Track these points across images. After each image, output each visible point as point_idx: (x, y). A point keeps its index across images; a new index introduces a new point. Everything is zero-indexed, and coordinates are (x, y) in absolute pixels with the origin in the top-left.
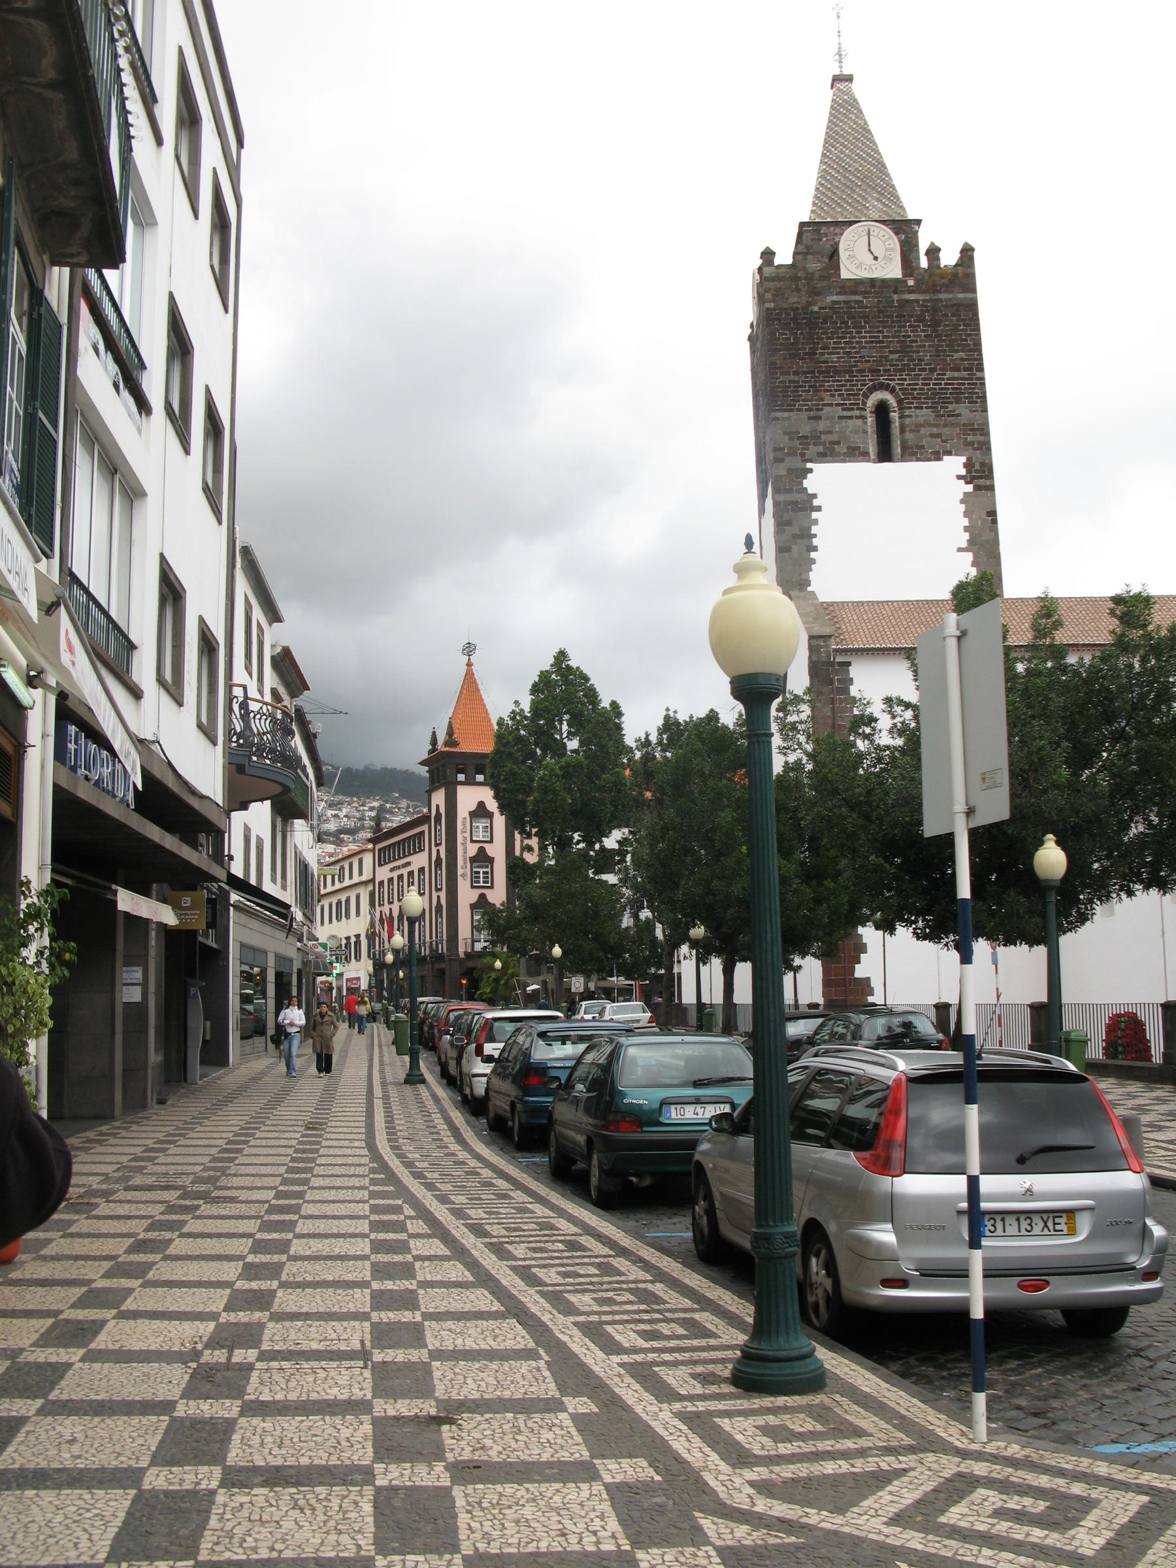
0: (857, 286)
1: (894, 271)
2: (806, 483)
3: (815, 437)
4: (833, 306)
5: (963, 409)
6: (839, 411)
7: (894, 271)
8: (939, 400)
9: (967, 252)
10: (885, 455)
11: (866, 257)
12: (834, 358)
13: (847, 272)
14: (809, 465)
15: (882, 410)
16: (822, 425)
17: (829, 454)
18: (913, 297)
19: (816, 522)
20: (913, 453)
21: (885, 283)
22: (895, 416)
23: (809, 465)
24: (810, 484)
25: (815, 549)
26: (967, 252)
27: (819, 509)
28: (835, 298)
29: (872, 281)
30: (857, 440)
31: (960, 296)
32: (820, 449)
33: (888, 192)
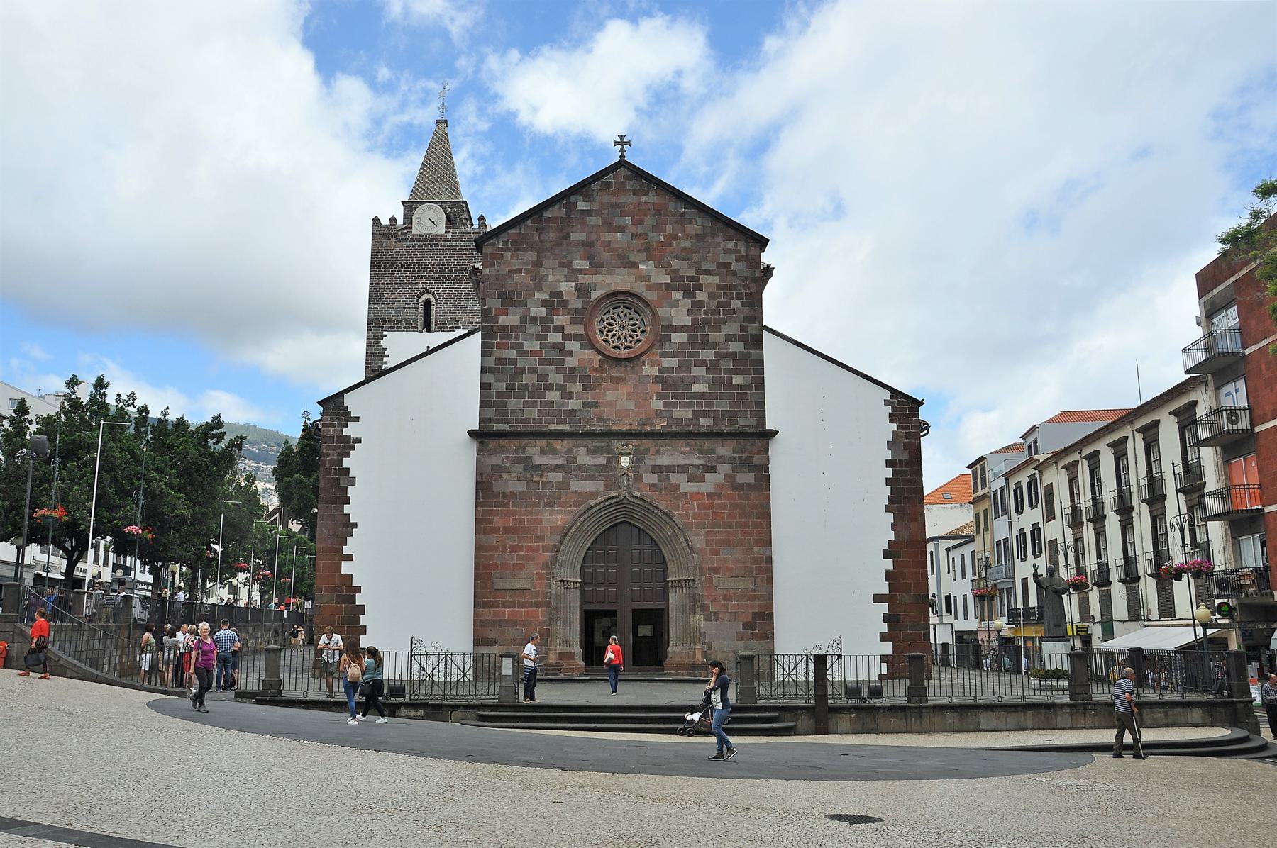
0: (423, 238)
1: (441, 230)
5: (469, 305)
7: (441, 230)
8: (456, 299)
9: (482, 219)
10: (427, 326)
11: (430, 222)
15: (427, 304)
17: (392, 329)
20: (441, 328)
21: (435, 239)
22: (433, 307)
26: (482, 219)
33: (453, 186)
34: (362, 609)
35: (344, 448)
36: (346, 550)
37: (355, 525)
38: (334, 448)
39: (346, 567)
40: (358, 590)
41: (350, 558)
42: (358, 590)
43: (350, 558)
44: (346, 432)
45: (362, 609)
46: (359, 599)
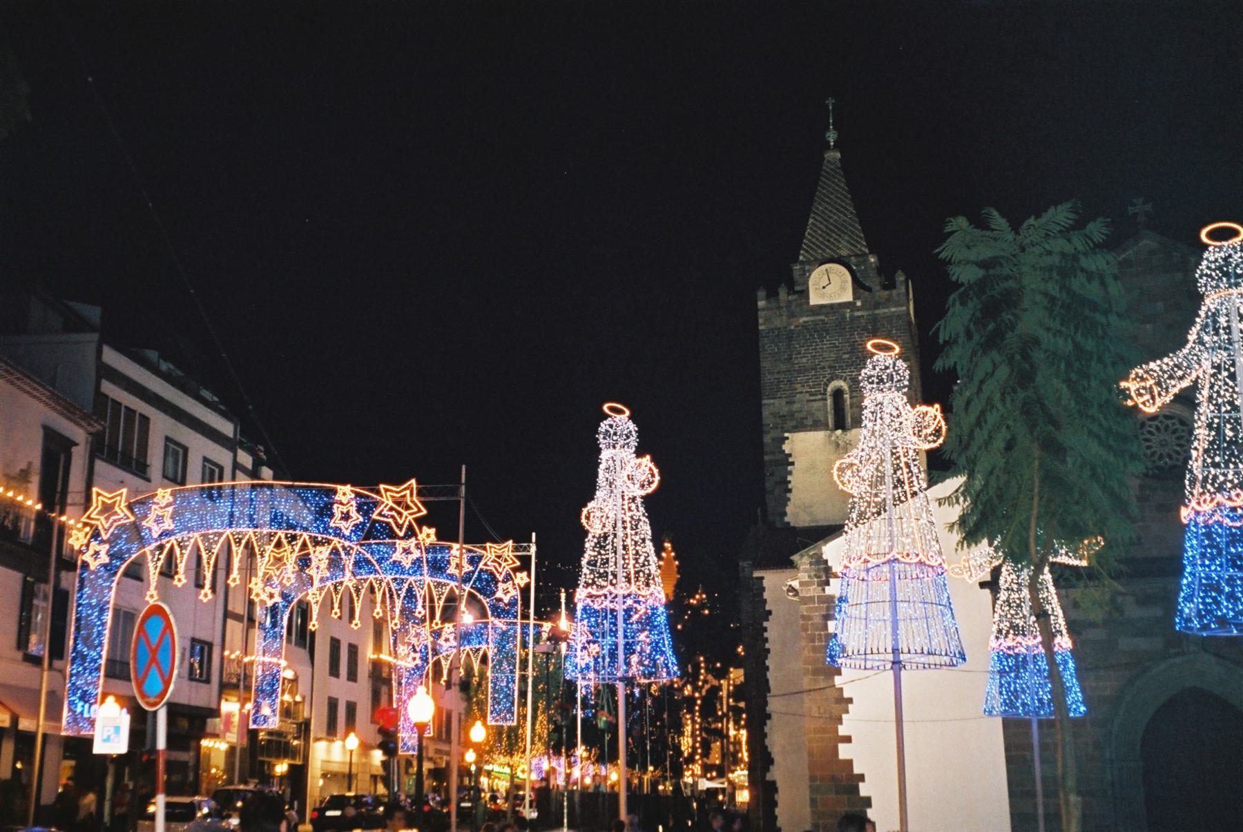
2: (784, 447)
3: (791, 415)
4: (805, 326)
6: (807, 397)
12: (804, 360)
13: (815, 300)
14: (786, 435)
16: (796, 407)
18: (859, 314)
19: (790, 473)
22: (847, 396)
23: (786, 435)
24: (786, 448)
25: (790, 491)
27: (793, 464)
28: (805, 319)
29: (832, 306)
30: (820, 416)
31: (893, 309)
32: (794, 423)
34: (867, 802)
35: (828, 609)
36: (843, 731)
37: (850, 700)
38: (816, 609)
39: (844, 752)
40: (861, 778)
41: (848, 739)
42: (861, 778)
43: (848, 739)
44: (829, 591)
45: (867, 802)
46: (864, 790)
